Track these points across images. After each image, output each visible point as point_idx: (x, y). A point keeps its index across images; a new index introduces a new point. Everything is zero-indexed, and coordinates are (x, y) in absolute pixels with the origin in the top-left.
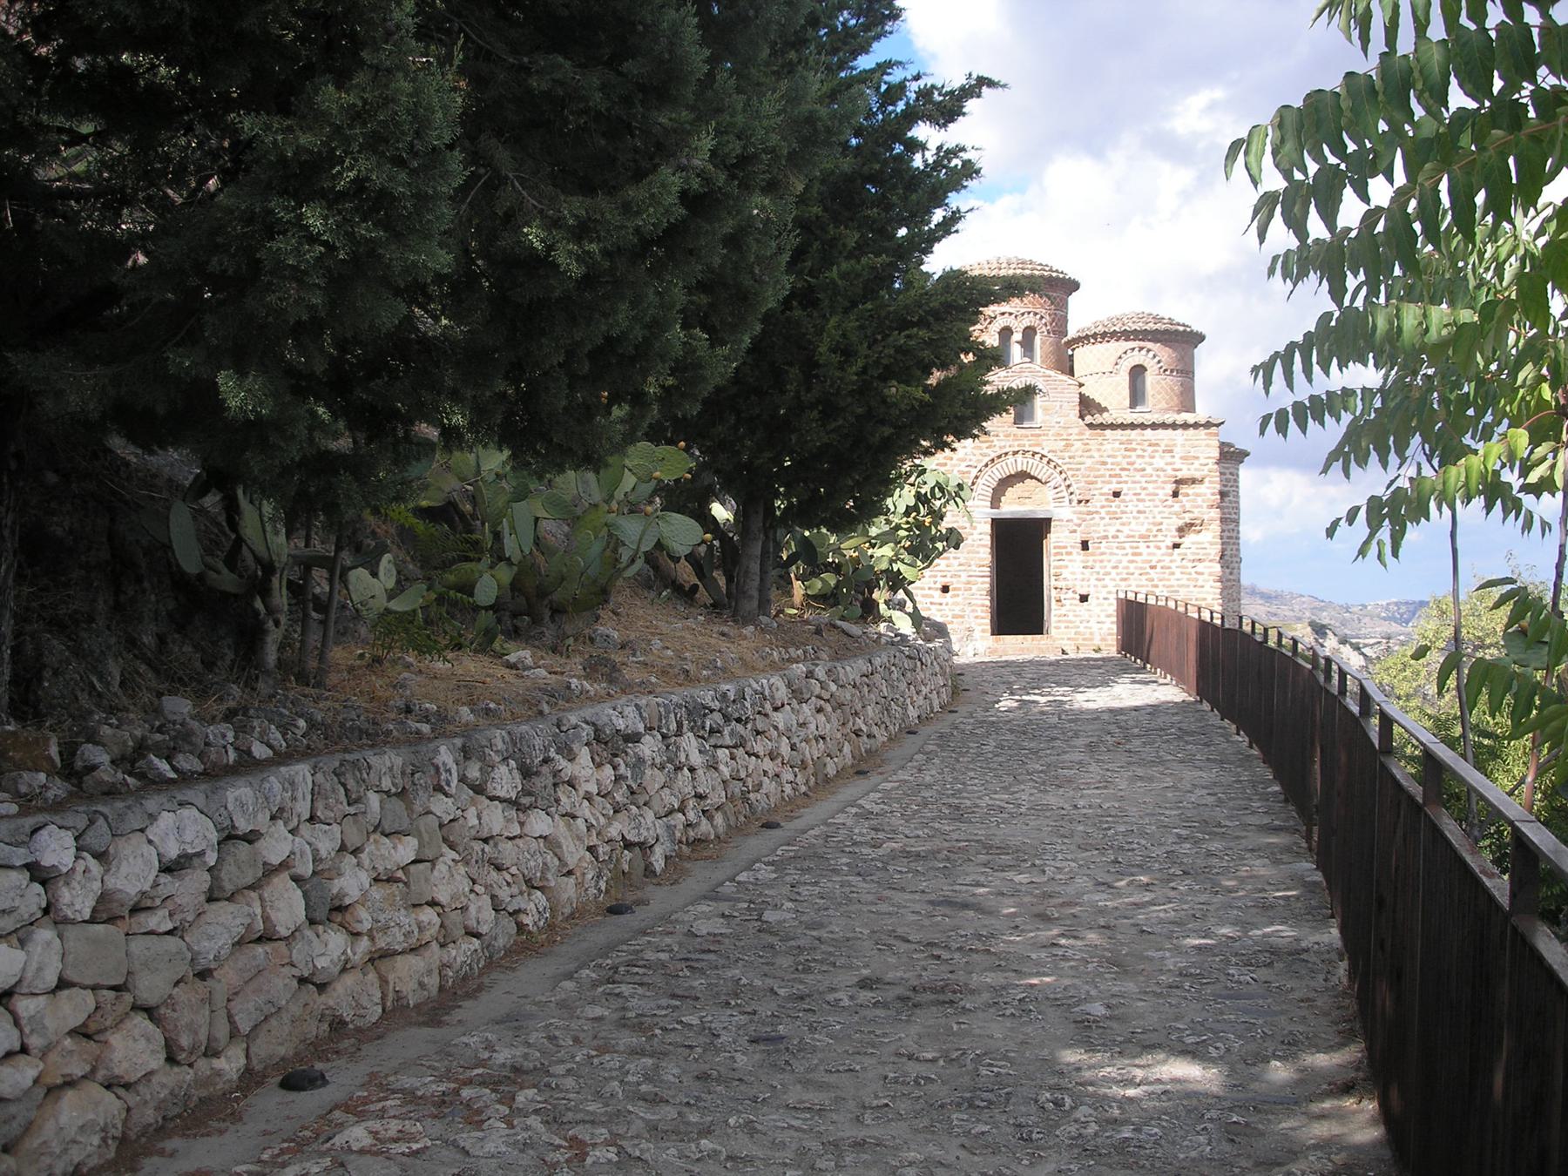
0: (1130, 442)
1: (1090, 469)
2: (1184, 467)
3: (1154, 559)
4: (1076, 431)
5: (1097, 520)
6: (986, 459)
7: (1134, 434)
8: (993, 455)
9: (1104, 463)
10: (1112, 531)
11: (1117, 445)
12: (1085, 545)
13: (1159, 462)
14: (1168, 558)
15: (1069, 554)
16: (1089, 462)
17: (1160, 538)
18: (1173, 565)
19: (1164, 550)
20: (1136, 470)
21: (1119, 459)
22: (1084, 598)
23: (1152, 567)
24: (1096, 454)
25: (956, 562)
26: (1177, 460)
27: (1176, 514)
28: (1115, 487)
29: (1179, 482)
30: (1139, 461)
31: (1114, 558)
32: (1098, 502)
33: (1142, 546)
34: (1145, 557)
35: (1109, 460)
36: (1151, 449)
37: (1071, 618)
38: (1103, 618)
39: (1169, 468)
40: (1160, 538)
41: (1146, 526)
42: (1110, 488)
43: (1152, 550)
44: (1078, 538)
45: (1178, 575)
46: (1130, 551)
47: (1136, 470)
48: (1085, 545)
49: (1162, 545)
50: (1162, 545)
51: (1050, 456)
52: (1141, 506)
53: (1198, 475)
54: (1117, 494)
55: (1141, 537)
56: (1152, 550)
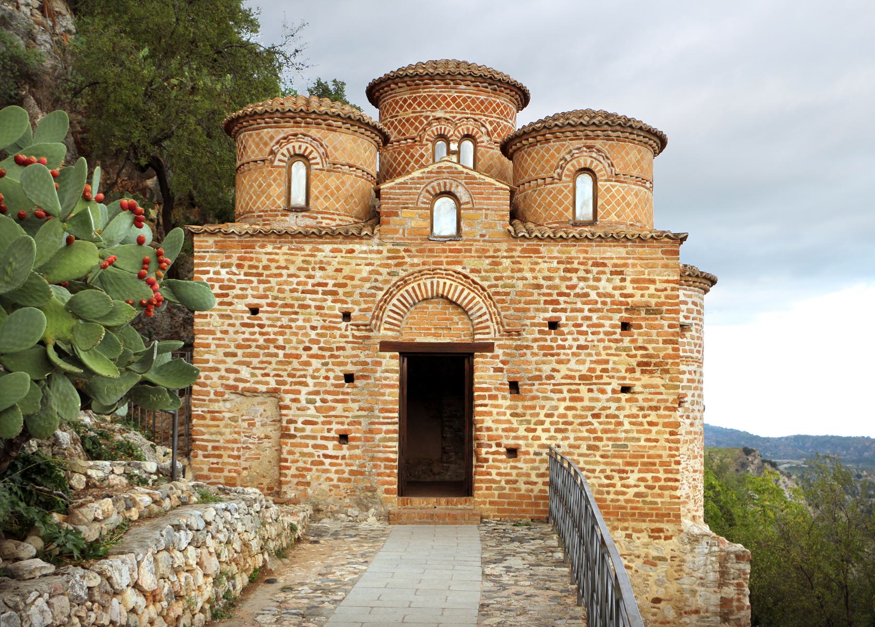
0: (569, 261)
1: (522, 294)
2: (639, 293)
3: (599, 405)
4: (504, 246)
5: (529, 357)
6: (395, 279)
7: (573, 252)
8: (403, 274)
9: (539, 286)
10: (546, 369)
11: (555, 264)
12: (514, 386)
13: (605, 286)
14: (614, 405)
15: (495, 397)
16: (520, 283)
17: (605, 380)
18: (621, 414)
19: (610, 395)
20: (577, 295)
21: (557, 281)
22: (512, 452)
23: (596, 416)
24: (529, 275)
25: (356, 406)
26: (627, 283)
27: (625, 349)
28: (549, 315)
29: (632, 309)
30: (582, 284)
31: (548, 404)
32: (530, 335)
33: (583, 388)
34: (586, 403)
35: (545, 283)
36: (595, 270)
37: (494, 477)
38: (534, 478)
39: (617, 293)
40: (605, 380)
41: (588, 365)
42: (543, 317)
43: (596, 394)
44: (504, 379)
45: (627, 426)
46: (566, 395)
47: (577, 295)
48: (514, 386)
49: (609, 388)
50: (609, 388)
51: (471, 276)
52: (582, 342)
53: (653, 301)
54: (553, 325)
55: (582, 377)
56: (596, 394)
